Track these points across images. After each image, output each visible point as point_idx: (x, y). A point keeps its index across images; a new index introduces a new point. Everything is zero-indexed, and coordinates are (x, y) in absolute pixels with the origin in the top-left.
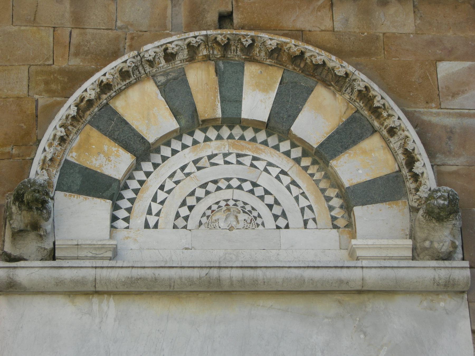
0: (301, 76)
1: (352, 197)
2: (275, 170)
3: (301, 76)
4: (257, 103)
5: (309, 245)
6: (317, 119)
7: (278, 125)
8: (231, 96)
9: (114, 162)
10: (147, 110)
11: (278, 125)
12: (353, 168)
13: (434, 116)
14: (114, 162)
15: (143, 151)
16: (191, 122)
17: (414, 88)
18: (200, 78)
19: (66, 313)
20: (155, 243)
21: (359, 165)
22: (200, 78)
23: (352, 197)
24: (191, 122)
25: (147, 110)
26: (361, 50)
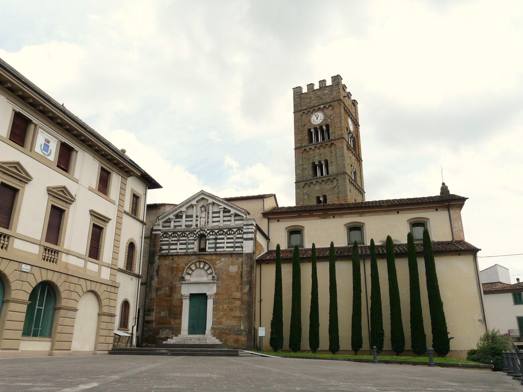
0: (205, 263)
1: (209, 274)
2: (203, 272)
3: (205, 263)
4: (202, 266)
5: (205, 279)
6: (206, 268)
7: (203, 268)
8: (200, 266)
9: (190, 272)
10: (193, 267)
11: (203, 268)
12: (209, 272)
13: (216, 267)
14: (190, 272)
15: (193, 271)
16: (197, 268)
17: (214, 264)
18: (197, 264)
19: (186, 285)
20: (193, 279)
21: (209, 272)
22: (197, 264)
23: (209, 274)
24: (197, 268)
25: (193, 267)
26: (211, 260)
